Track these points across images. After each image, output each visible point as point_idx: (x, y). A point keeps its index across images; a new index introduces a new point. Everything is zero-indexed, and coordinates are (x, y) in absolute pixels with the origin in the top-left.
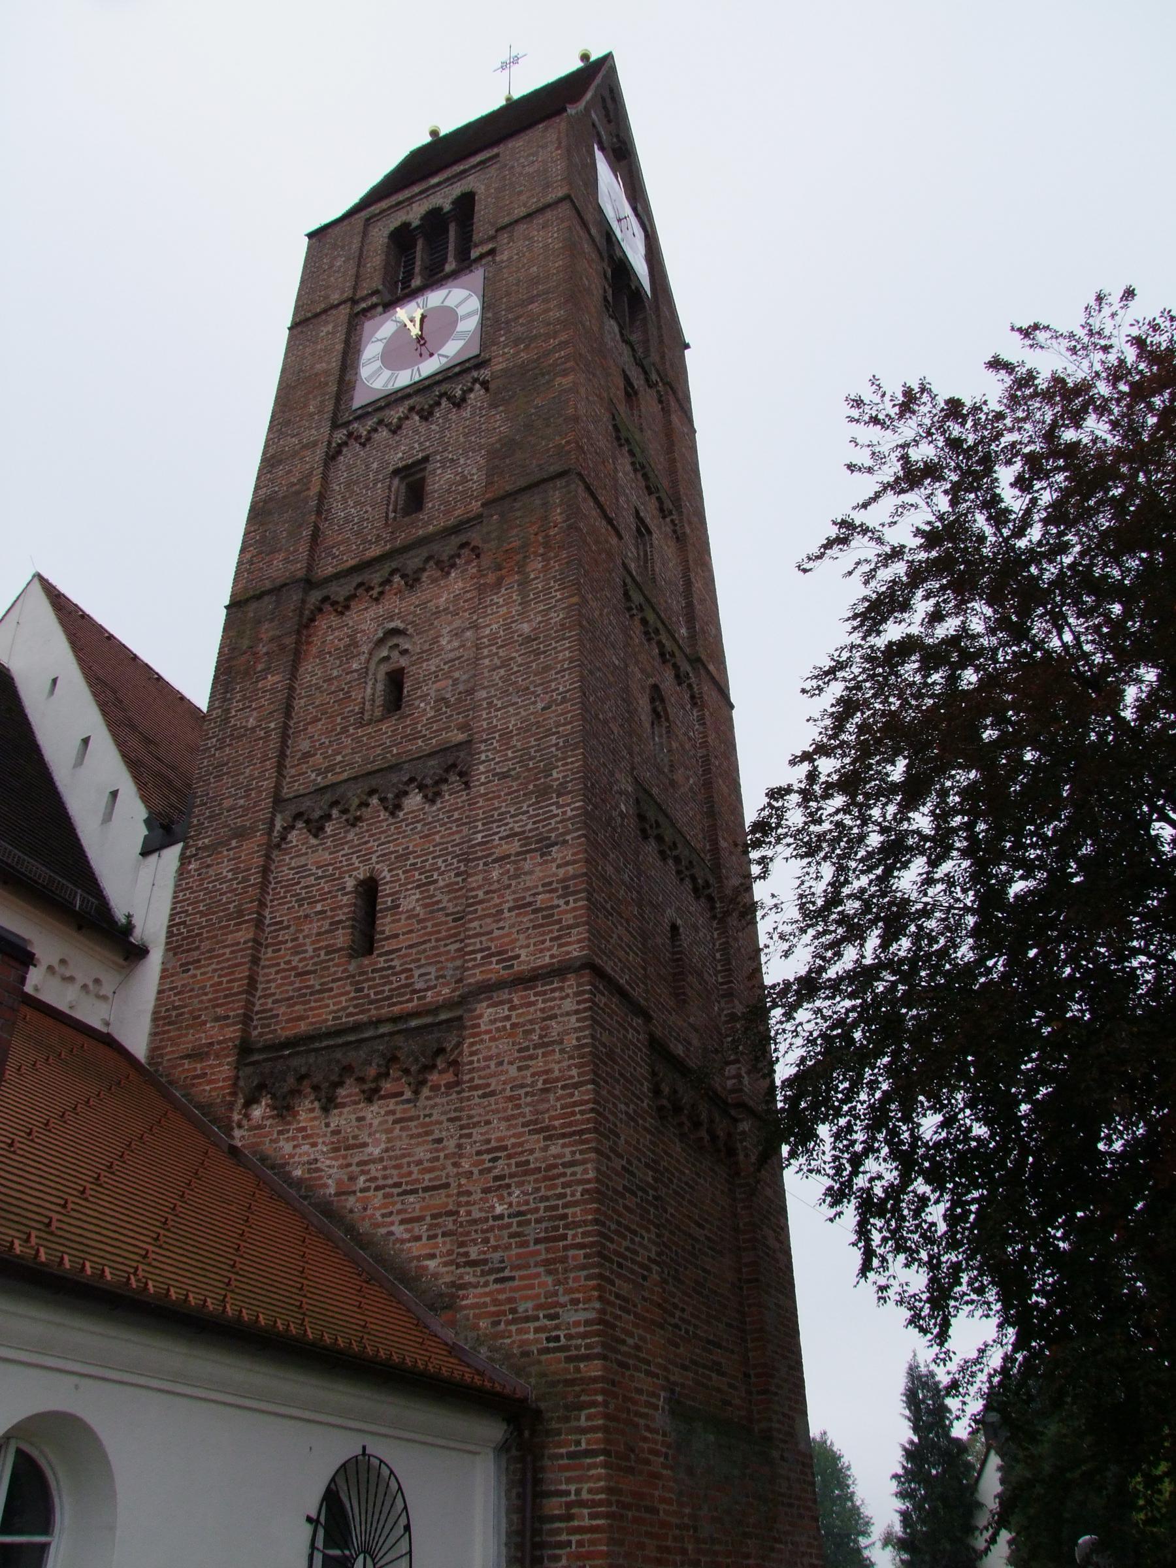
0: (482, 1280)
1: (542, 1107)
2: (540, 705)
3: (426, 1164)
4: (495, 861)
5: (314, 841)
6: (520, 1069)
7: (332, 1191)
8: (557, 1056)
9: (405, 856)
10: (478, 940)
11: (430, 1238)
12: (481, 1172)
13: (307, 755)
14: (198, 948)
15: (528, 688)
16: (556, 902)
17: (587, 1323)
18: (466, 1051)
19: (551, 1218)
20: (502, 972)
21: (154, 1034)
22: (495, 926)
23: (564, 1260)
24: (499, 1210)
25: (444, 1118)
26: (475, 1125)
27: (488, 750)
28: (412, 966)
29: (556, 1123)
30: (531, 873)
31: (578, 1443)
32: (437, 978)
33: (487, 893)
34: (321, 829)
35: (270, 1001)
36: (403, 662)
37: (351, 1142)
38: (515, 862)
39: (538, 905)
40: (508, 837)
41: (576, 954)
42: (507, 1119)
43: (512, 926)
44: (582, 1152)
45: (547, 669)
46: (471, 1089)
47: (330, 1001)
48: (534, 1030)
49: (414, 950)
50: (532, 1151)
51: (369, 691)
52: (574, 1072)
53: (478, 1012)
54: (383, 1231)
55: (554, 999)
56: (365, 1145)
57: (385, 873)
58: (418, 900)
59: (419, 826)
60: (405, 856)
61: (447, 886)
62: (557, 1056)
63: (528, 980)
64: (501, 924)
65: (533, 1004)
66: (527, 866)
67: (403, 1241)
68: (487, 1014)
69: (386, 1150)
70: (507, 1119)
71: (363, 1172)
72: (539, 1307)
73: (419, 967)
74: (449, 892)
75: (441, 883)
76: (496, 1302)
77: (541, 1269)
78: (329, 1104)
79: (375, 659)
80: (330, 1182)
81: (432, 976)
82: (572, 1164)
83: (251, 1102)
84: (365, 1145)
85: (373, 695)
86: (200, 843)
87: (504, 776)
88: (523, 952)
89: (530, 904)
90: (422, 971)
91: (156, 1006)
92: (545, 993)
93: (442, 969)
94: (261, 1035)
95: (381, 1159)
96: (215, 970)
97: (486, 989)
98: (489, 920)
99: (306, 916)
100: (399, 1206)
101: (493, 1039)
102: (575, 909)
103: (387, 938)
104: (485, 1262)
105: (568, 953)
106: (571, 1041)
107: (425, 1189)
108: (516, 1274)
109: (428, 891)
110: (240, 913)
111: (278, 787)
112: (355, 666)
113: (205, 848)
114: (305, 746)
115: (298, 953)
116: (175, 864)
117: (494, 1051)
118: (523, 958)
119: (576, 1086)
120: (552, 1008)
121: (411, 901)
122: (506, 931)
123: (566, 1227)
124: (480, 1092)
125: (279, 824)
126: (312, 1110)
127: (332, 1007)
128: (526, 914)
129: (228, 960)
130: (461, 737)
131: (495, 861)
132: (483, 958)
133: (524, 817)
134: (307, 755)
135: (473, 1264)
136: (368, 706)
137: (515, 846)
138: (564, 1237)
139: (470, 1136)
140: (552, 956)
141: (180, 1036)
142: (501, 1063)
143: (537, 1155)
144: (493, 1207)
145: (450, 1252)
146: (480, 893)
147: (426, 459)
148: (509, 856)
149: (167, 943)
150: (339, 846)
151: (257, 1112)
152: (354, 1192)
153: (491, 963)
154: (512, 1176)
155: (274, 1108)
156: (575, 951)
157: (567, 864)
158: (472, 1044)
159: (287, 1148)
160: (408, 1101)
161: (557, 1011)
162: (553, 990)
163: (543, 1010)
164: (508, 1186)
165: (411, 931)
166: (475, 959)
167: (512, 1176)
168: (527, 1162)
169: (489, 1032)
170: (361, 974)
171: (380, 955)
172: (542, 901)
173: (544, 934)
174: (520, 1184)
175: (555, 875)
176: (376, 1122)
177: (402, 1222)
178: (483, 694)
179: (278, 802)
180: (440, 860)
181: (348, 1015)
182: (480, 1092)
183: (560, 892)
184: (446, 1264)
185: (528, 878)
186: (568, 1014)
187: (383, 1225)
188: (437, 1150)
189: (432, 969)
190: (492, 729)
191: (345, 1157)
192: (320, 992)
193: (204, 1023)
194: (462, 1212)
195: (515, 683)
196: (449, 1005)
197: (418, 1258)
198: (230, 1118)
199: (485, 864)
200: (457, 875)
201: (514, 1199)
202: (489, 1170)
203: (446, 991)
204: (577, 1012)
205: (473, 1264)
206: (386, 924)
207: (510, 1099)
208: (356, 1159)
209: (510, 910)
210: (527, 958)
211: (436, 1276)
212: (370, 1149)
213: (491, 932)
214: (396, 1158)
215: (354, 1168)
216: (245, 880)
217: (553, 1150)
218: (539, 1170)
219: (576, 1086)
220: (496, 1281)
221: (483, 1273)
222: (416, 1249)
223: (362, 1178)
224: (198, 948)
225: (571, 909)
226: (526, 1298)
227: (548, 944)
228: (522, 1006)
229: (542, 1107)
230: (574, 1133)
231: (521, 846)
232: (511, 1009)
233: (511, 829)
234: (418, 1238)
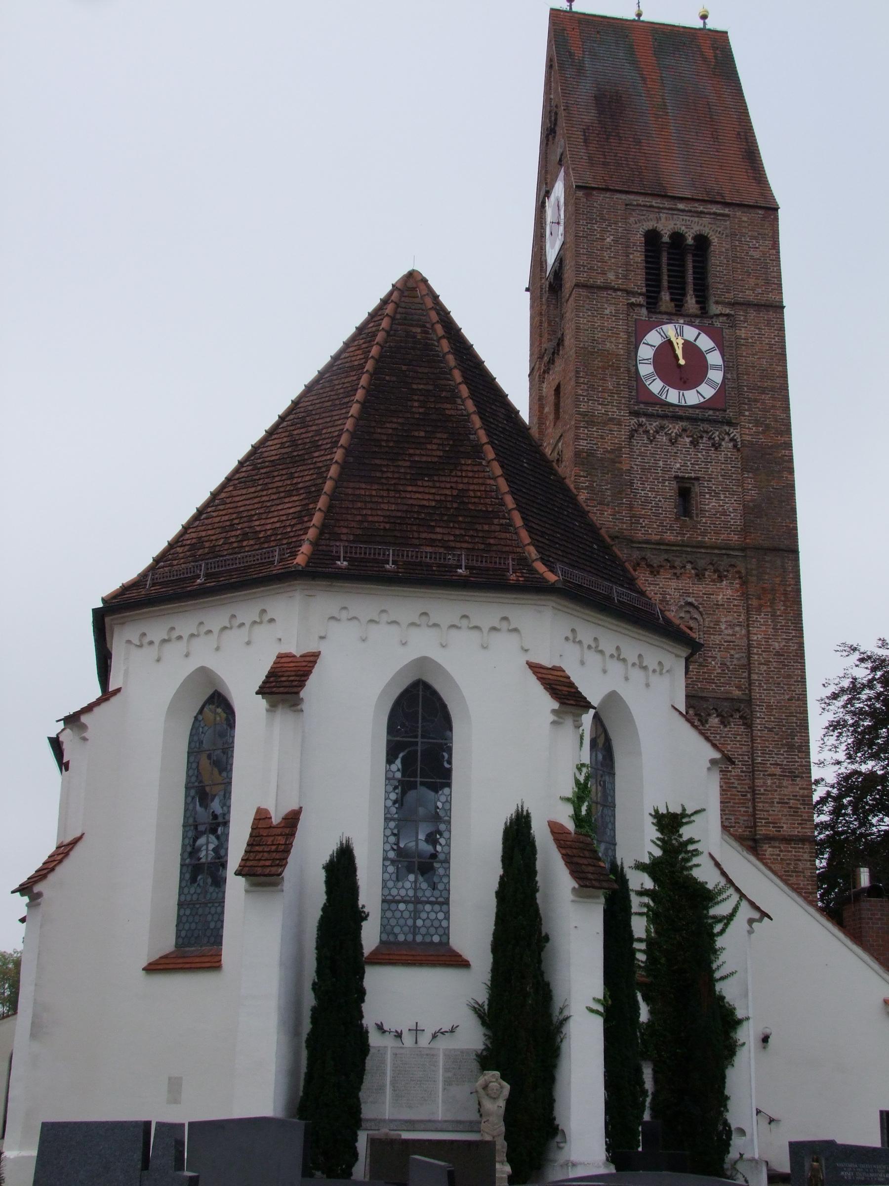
2: (787, 697)
15: (779, 684)
16: (799, 806)
20: (775, 833)
30: (787, 787)
39: (791, 805)
43: (779, 811)
48: (791, 864)
52: (810, 887)
53: (764, 848)
55: (800, 852)
64: (773, 809)
88: (785, 826)
98: (767, 805)
105: (806, 833)
118: (784, 829)
120: (799, 856)
122: (776, 812)
128: (786, 807)
137: (778, 771)
140: (798, 832)
148: (775, 775)
162: (799, 848)
166: (761, 822)
185: (785, 789)
190: (762, 700)
227: (796, 825)
231: (781, 772)
233: (776, 761)
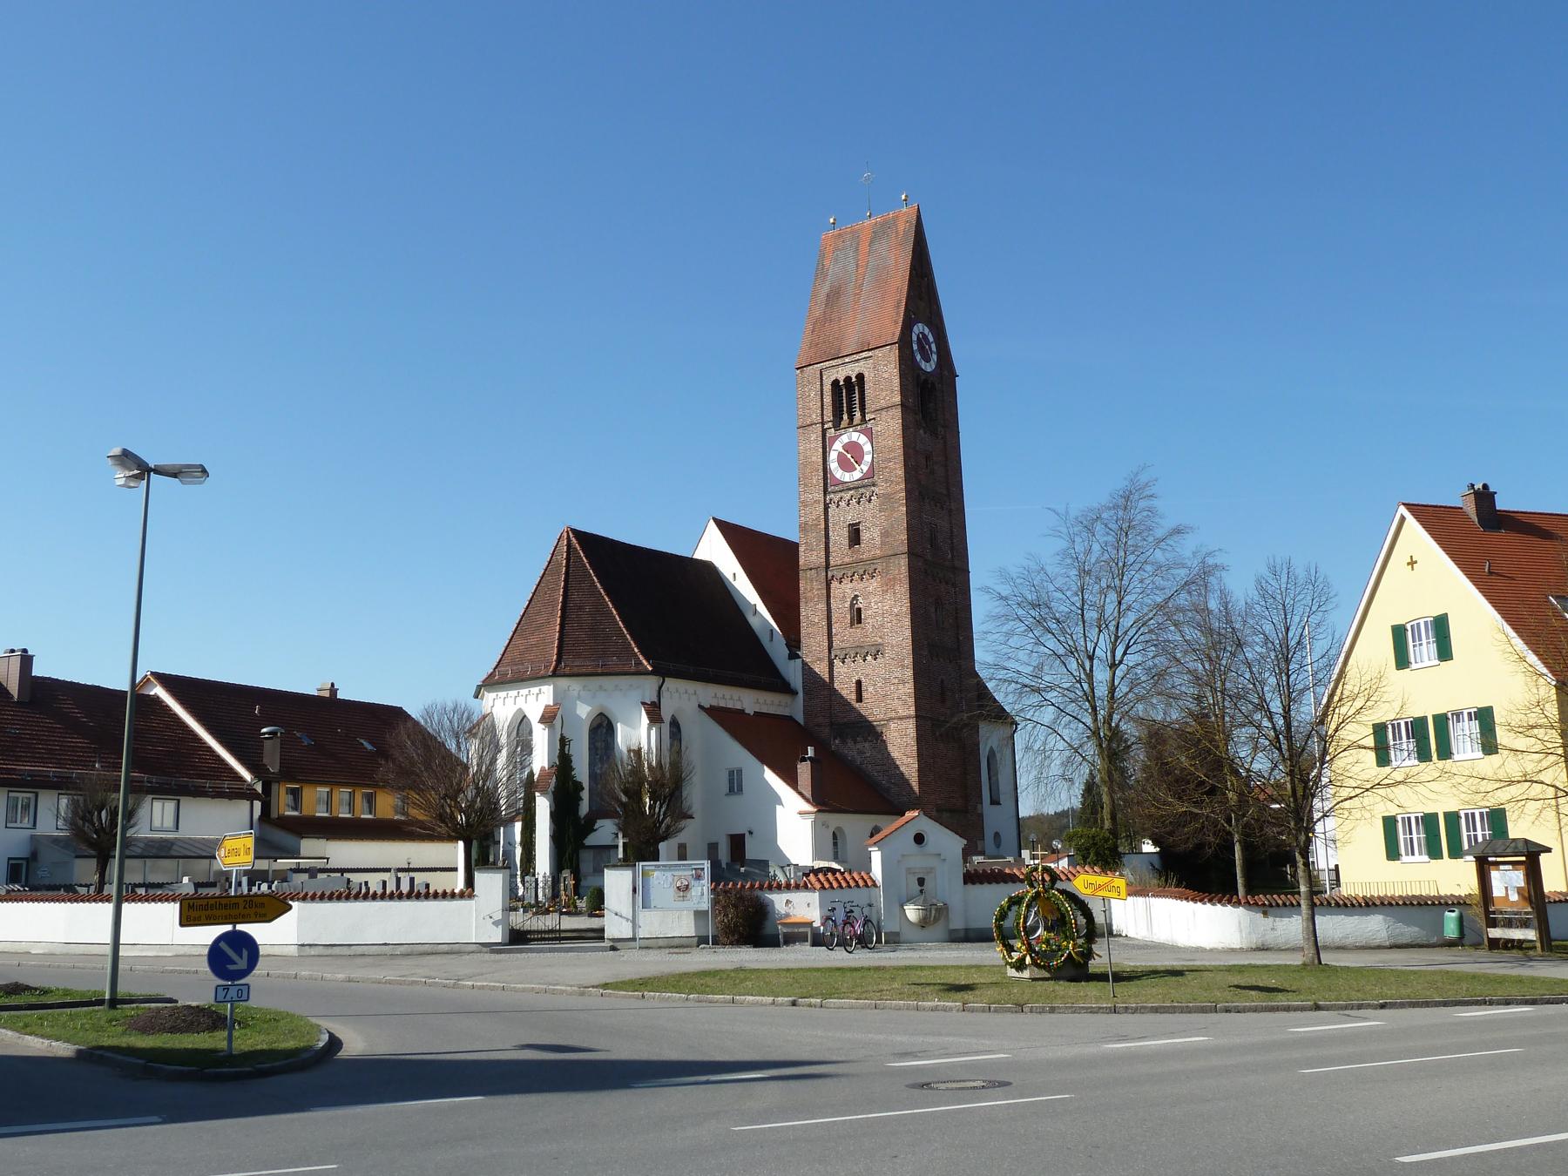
63: (900, 718)
68: (893, 725)
87: (893, 659)
121: (870, 689)
137: (896, 681)
147: (860, 522)
151: (837, 741)
210: (902, 713)
222: (880, 778)
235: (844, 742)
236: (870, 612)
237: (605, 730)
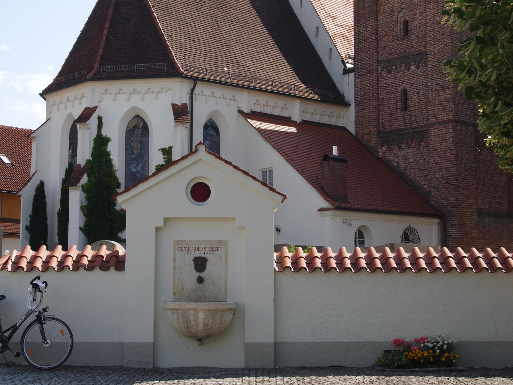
0: (435, 191)
1: (446, 154)
2: (443, 46)
3: (423, 164)
4: (433, 91)
5: (389, 76)
6: (441, 145)
7: (403, 169)
8: (448, 143)
9: (412, 84)
10: (430, 112)
11: (424, 181)
12: (434, 168)
13: (384, 48)
14: (363, 105)
15: (439, 40)
16: (447, 104)
17: (455, 200)
18: (429, 139)
19: (448, 179)
20: (436, 121)
21: (356, 128)
22: (434, 109)
23: (450, 187)
24: (437, 176)
25: (426, 154)
26: (432, 157)
27: (430, 58)
28: (416, 115)
29: (448, 158)
30: (442, 95)
31: (453, 223)
32: (422, 119)
33: (432, 99)
34: (391, 72)
35: (384, 120)
36: (408, 18)
37: (406, 158)
38: (438, 92)
40: (436, 84)
41: (452, 118)
42: (438, 156)
43: (438, 109)
44: (453, 165)
45: (444, 34)
46: (431, 149)
47: (398, 122)
48: (443, 136)
49: (417, 111)
50: (443, 164)
51: (399, 28)
52: (452, 147)
53: (431, 130)
54: (414, 178)
55: (447, 129)
56: (409, 159)
57: (408, 88)
58: (416, 97)
59: (415, 75)
60: (412, 84)
61: (423, 94)
62: (448, 143)
63: (441, 123)
64: (435, 108)
65: (443, 130)
66: (441, 93)
67: (419, 181)
68: (433, 131)
69: (414, 160)
70: (438, 156)
71: (409, 165)
72: (445, 197)
73: (418, 116)
74: (424, 96)
75: (422, 93)
76: (437, 195)
77: (446, 189)
78: (400, 148)
79: (399, 17)
80: (402, 167)
81: (421, 118)
82: (450, 168)
83: (382, 146)
84: (409, 159)
85: (400, 29)
86: (359, 73)
87: (434, 66)
88: (440, 116)
89: (442, 104)
90: (419, 117)
91: (355, 120)
92: (445, 127)
93: (424, 117)
94: (382, 129)
95: (413, 162)
96: (369, 112)
97: (432, 124)
98: (433, 107)
99: (390, 98)
100: (417, 173)
101: (435, 137)
102: (452, 107)
103: (410, 107)
104: (435, 187)
105: (450, 118)
106: (451, 139)
107: (423, 170)
108: (441, 190)
109: (419, 95)
110: (373, 96)
111: (378, 59)
112: (394, 19)
113: (361, 75)
114: (383, 44)
115: (389, 108)
116: (353, 79)
117: (435, 140)
119: (452, 150)
120: (447, 131)
121: (415, 97)
122: (437, 110)
123: (450, 181)
124: (433, 150)
125: (379, 69)
126: (397, 150)
127: (398, 124)
128: (441, 106)
129: (372, 109)
130: (424, 49)
131: (433, 91)
132: (432, 117)
133: (439, 79)
134: (384, 48)
135: (432, 187)
136: (399, 33)
138: (450, 183)
139: (431, 159)
140: (447, 118)
141: (362, 129)
142: (436, 143)
143: (444, 165)
144: (436, 176)
145: (428, 184)
146: (430, 99)
148: (436, 90)
149: (355, 103)
150: (396, 78)
151: (384, 149)
152: (408, 169)
153: (433, 118)
154: (440, 169)
155: (387, 148)
156: (451, 117)
157: (449, 94)
158: (430, 138)
159: (392, 158)
160: (418, 149)
161: (448, 132)
162: (447, 127)
163: (445, 131)
164: (439, 171)
165: (415, 106)
166: (430, 117)
167: (440, 169)
168: (442, 166)
169: (434, 135)
170: (405, 116)
171: (409, 111)
172: (444, 104)
173: (445, 112)
174: (441, 171)
175: (447, 97)
176: (411, 154)
177: (418, 177)
178: (428, 39)
179: (378, 62)
180: (421, 86)
181: (403, 126)
182: (433, 150)
183: (448, 102)
184: (428, 186)
186: (450, 133)
187: (414, 177)
188: (425, 161)
189: (421, 116)
191: (405, 161)
192: (395, 119)
193: (368, 126)
194: (430, 176)
195: (436, 37)
196: (425, 126)
197: (422, 185)
198: (378, 151)
199: (431, 91)
200: (425, 91)
201: (440, 174)
202: (435, 167)
203: (424, 123)
204: (452, 133)
205: (432, 187)
206: (409, 103)
207: (439, 152)
208: (407, 162)
209: (437, 105)
210: (442, 117)
211: (426, 189)
212: (410, 160)
213: (433, 110)
214: (416, 162)
215: (407, 164)
216: (373, 87)
217: (448, 164)
218: (445, 168)
219: (452, 150)
220: (437, 191)
221: (435, 189)
222: (422, 183)
223: (409, 166)
224: (363, 105)
225: (450, 106)
226: (443, 195)
227: (446, 115)
228: (441, 130)
229: (446, 154)
230: (452, 161)
231: (439, 88)
232: (438, 130)
233: (437, 82)
234: (422, 181)
235: (389, 149)
236: (415, 23)
237: (140, 131)
